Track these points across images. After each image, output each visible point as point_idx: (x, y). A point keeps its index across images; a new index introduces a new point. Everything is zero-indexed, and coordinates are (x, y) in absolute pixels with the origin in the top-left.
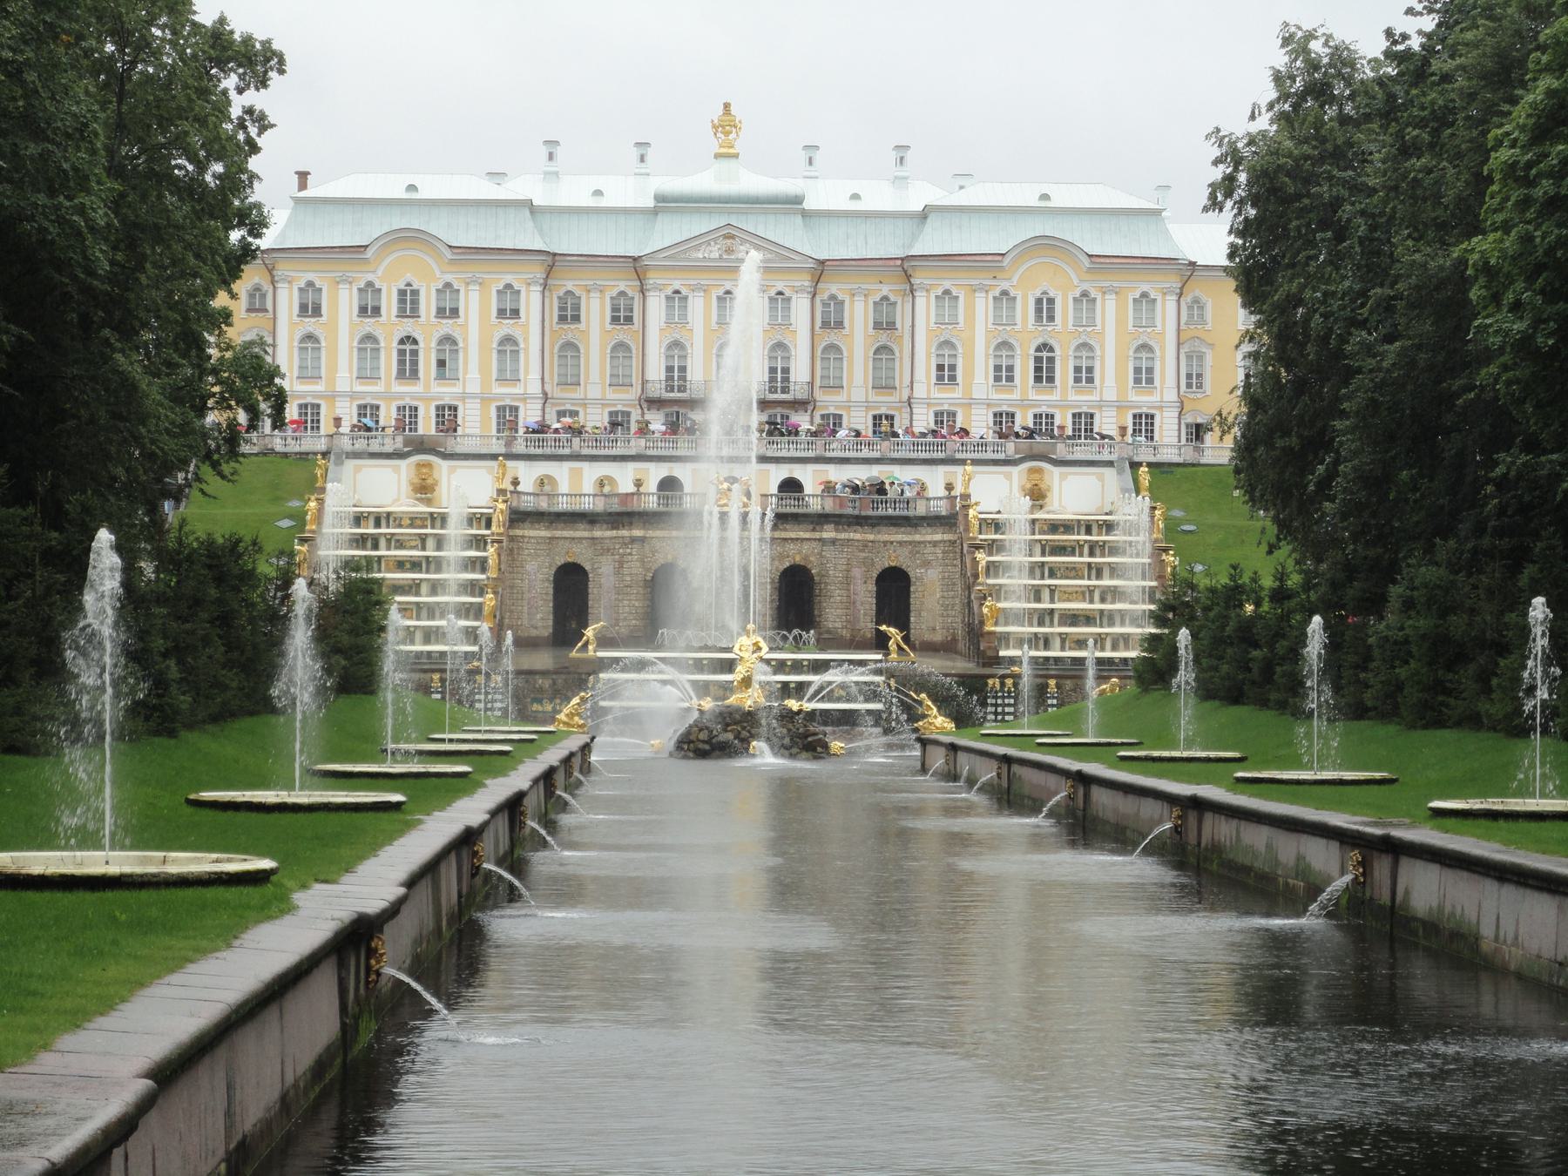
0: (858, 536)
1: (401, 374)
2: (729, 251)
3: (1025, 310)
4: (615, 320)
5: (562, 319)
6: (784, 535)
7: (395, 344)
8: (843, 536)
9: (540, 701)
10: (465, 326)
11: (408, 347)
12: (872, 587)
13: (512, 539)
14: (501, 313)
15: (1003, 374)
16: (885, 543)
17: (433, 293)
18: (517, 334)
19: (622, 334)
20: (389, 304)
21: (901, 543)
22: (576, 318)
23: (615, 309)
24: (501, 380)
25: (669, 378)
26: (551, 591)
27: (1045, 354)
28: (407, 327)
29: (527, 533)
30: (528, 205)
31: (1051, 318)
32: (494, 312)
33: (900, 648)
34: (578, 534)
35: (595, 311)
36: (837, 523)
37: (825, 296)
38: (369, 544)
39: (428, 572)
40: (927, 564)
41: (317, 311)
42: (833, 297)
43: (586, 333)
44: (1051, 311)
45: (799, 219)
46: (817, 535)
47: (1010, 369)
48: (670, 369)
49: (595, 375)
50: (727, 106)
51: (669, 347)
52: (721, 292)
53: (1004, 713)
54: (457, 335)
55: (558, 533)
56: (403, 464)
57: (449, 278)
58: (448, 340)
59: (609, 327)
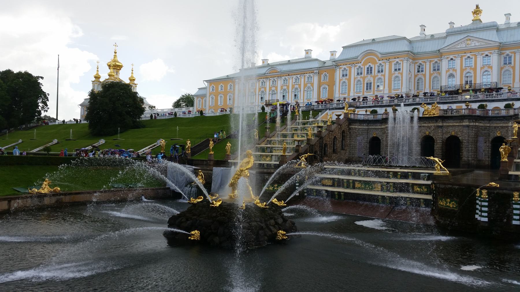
0: (481, 125)
1: (367, 89)
4: (434, 70)
5: (418, 71)
6: (447, 124)
10: (384, 76)
13: (350, 129)
14: (396, 70)
16: (495, 127)
17: (376, 67)
18: (400, 75)
21: (502, 127)
22: (422, 71)
24: (395, 90)
26: (368, 146)
29: (356, 127)
30: (405, 38)
32: (393, 70)
33: (441, 167)
34: (377, 127)
35: (428, 68)
36: (469, 119)
37: (505, 55)
42: (508, 55)
43: (425, 75)
45: (495, 31)
46: (461, 124)
50: (477, 7)
52: (466, 57)
53: (481, 211)
54: (382, 77)
55: (371, 127)
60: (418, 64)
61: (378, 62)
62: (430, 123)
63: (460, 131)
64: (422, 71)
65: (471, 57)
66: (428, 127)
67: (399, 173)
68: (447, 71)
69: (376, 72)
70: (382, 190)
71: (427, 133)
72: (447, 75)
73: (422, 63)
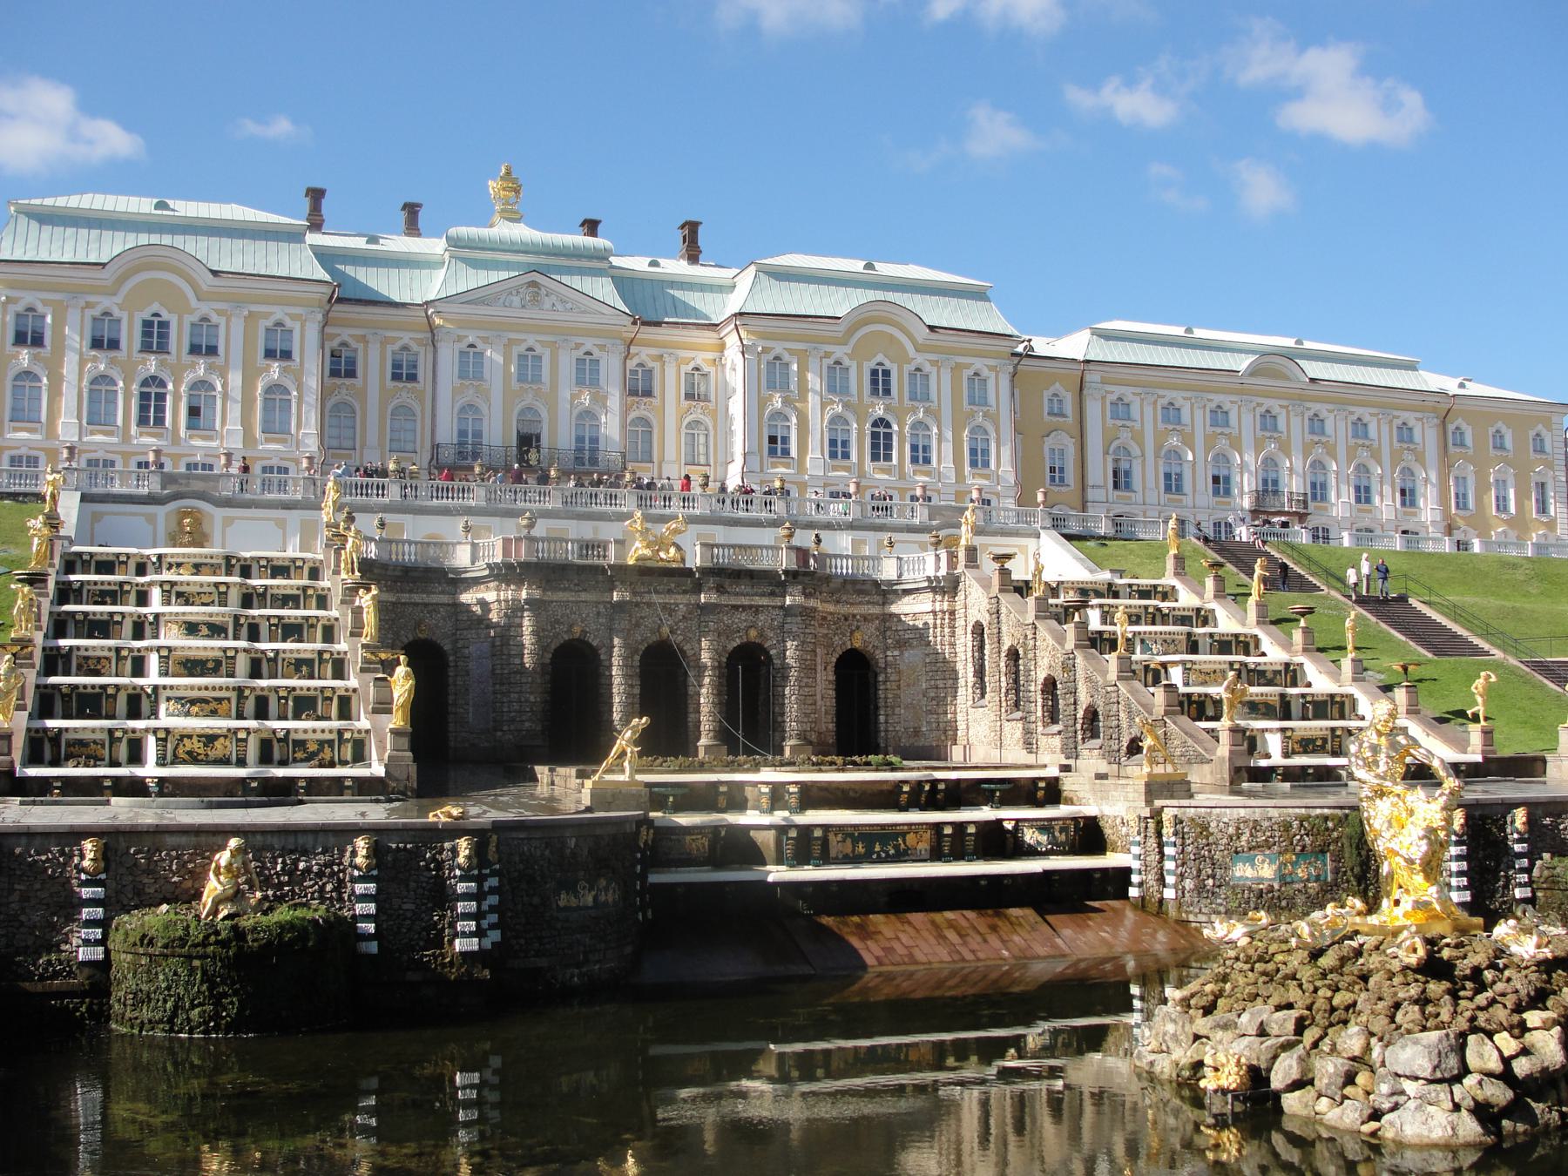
2: (536, 300)
3: (858, 380)
4: (396, 377)
5: (335, 373)
6: (734, 601)
7: (135, 387)
8: (812, 603)
9: (571, 887)
11: (153, 390)
12: (832, 677)
15: (838, 449)
19: (404, 394)
20: (131, 336)
21: (865, 618)
22: (351, 373)
23: (397, 365)
25: (461, 444)
27: (882, 430)
28: (152, 365)
31: (887, 392)
34: (435, 599)
35: (374, 366)
37: (635, 361)
38: (133, 597)
39: (236, 638)
40: (902, 644)
41: (38, 341)
43: (362, 394)
44: (887, 383)
46: (777, 602)
47: (845, 443)
48: (462, 433)
49: (372, 436)
51: (462, 410)
52: (522, 349)
55: (405, 597)
56: (160, 511)
57: (205, 308)
58: (201, 385)
59: (390, 384)
60: (335, 343)
61: (193, 302)
62: (670, 591)
63: (771, 628)
64: (351, 373)
65: (539, 350)
66: (665, 607)
67: (906, 788)
68: (455, 392)
69: (186, 347)
70: (936, 855)
71: (665, 630)
72: (458, 406)
73: (354, 344)
